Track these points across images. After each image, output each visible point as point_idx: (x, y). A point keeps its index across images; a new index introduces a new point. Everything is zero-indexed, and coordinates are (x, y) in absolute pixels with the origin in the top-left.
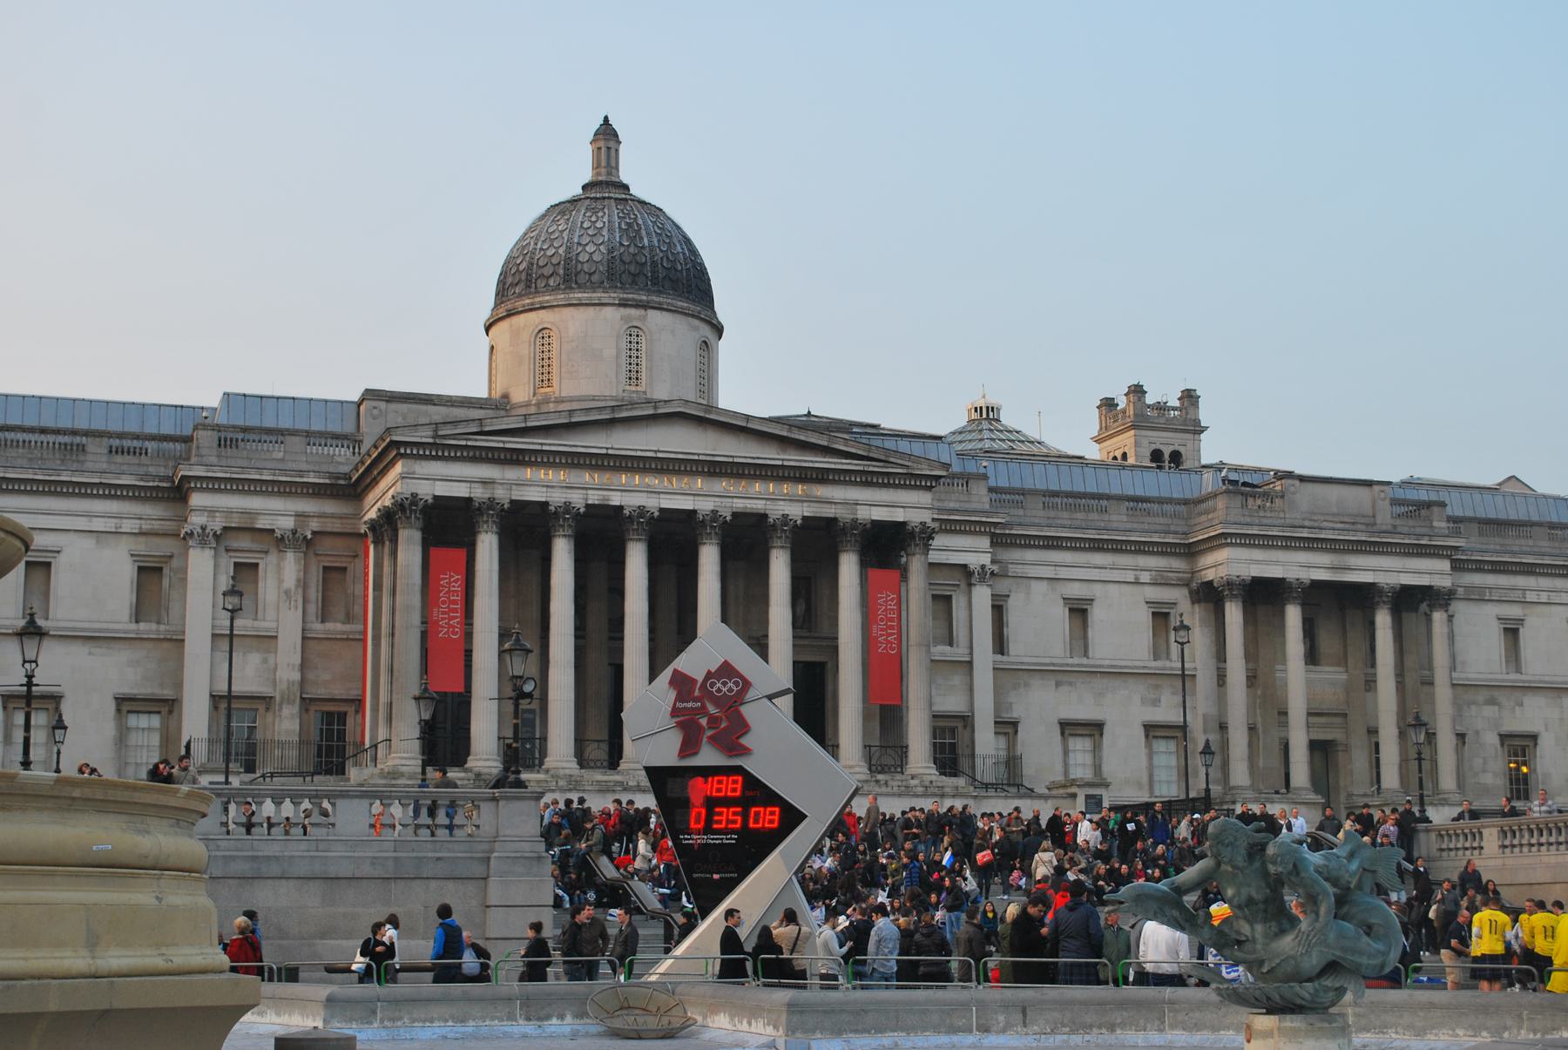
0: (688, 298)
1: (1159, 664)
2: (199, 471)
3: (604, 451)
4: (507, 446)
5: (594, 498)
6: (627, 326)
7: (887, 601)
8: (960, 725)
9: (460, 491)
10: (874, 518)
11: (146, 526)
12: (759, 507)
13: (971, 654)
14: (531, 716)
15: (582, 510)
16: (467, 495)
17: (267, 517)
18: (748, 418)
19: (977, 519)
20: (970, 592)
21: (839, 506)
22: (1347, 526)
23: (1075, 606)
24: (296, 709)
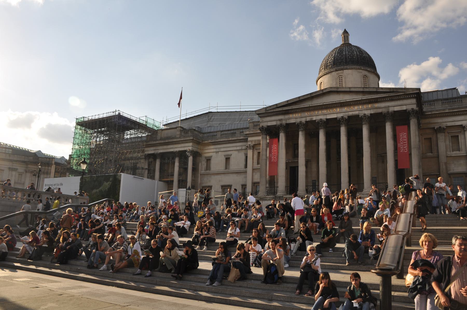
0: (357, 65)
2: (248, 133)
3: (309, 106)
4: (283, 109)
5: (308, 119)
6: (338, 76)
7: (403, 136)
9: (274, 123)
10: (395, 110)
12: (357, 113)
14: (315, 182)
18: (350, 88)
19: (464, 110)
20: (465, 133)
21: (383, 109)
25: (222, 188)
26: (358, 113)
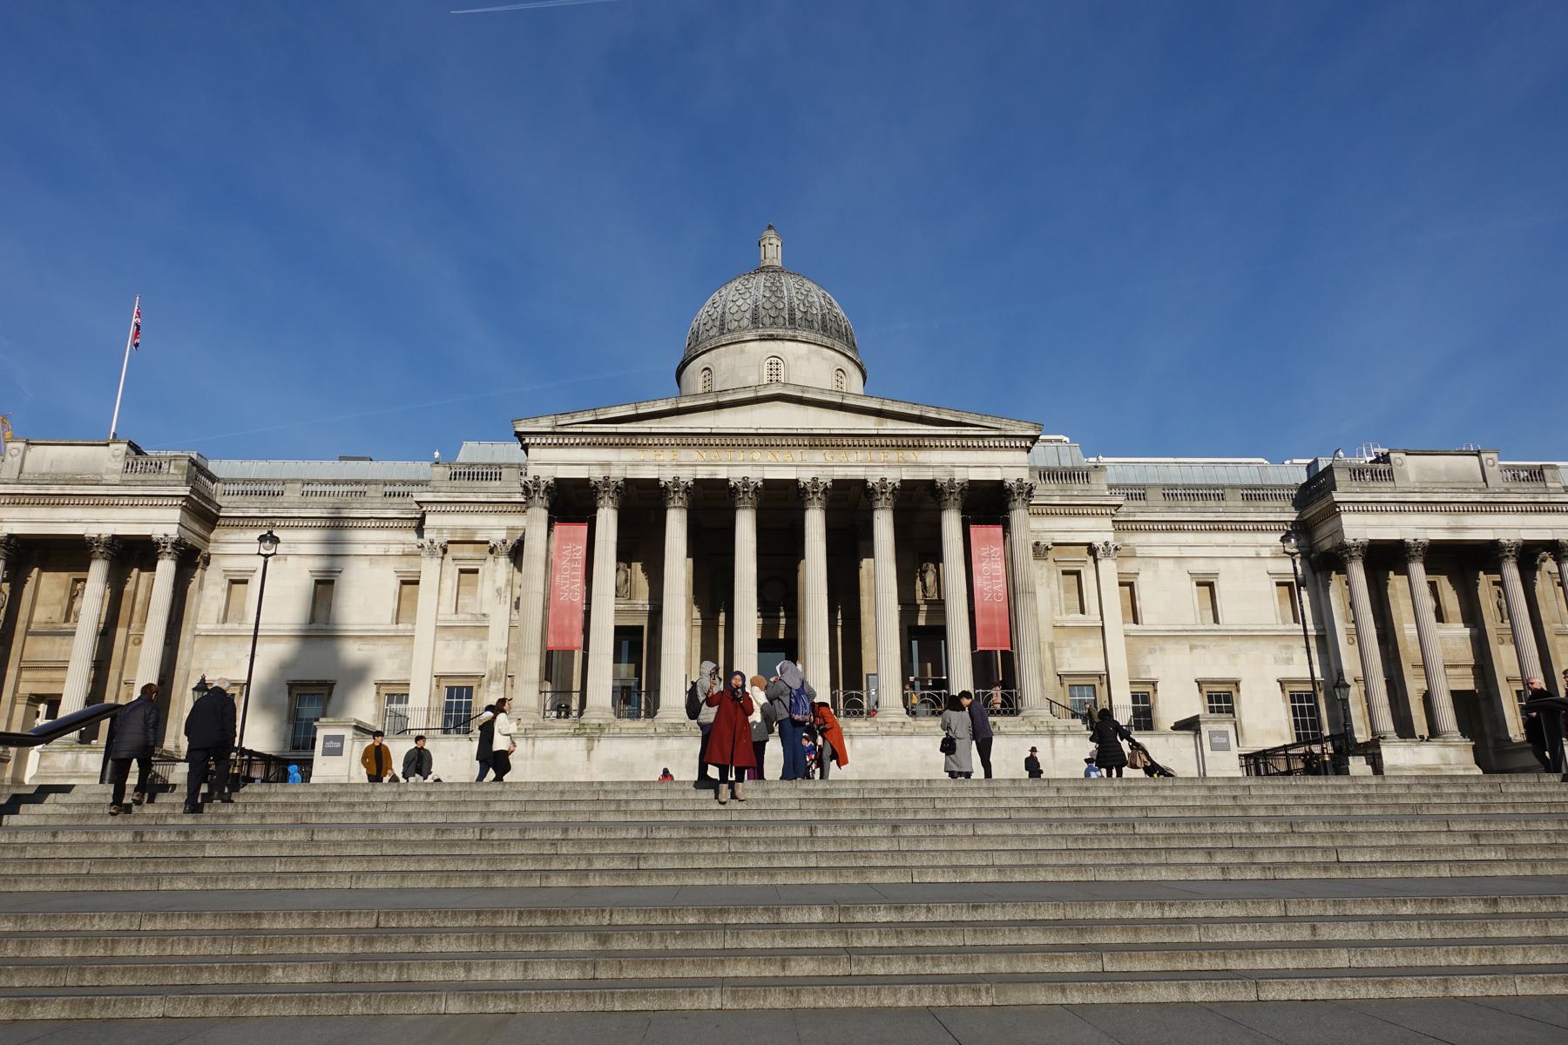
0: (823, 335)
1: (1288, 627)
3: (708, 431)
4: (619, 430)
5: (703, 473)
7: (990, 554)
8: (1097, 683)
10: (972, 478)
11: (407, 550)
13: (1102, 619)
15: (689, 484)
16: (587, 477)
17: (485, 531)
19: (1098, 502)
22: (1460, 491)
23: (1201, 580)
24: (502, 684)
25: (290, 693)
26: (863, 473)
